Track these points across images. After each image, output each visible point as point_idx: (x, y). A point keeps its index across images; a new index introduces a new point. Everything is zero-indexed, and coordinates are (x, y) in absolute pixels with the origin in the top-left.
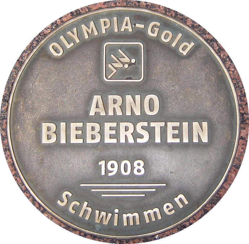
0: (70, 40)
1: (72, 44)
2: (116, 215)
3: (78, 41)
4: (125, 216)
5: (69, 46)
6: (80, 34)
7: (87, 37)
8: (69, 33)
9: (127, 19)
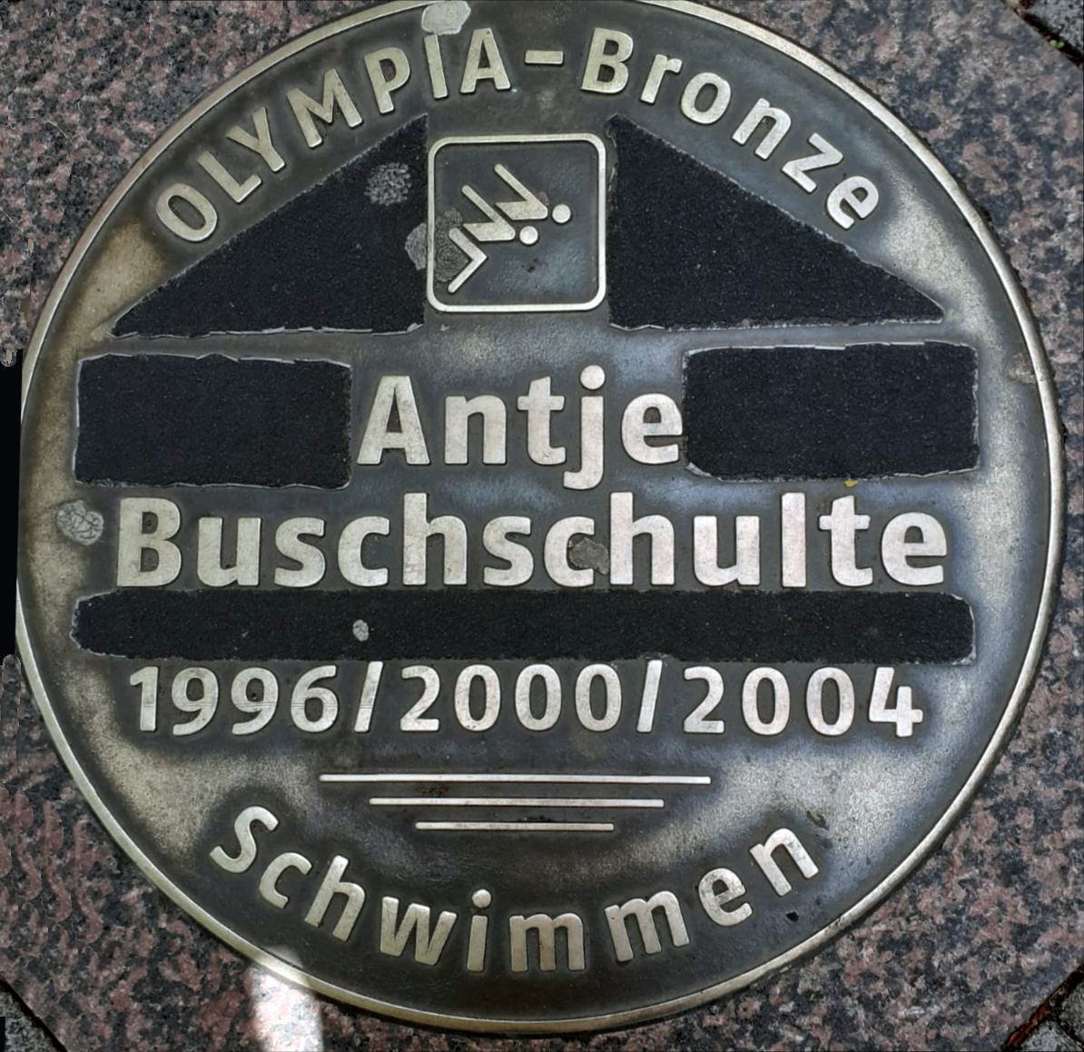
0: (242, 163)
2: (479, 922)
4: (518, 923)
5: (240, 193)
7: (314, 140)
8: (238, 134)
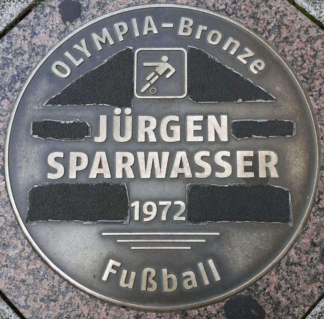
0: (77, 54)
1: (82, 60)
3: (89, 55)
5: (77, 63)
6: (90, 45)
8: (76, 46)
9: (149, 19)
